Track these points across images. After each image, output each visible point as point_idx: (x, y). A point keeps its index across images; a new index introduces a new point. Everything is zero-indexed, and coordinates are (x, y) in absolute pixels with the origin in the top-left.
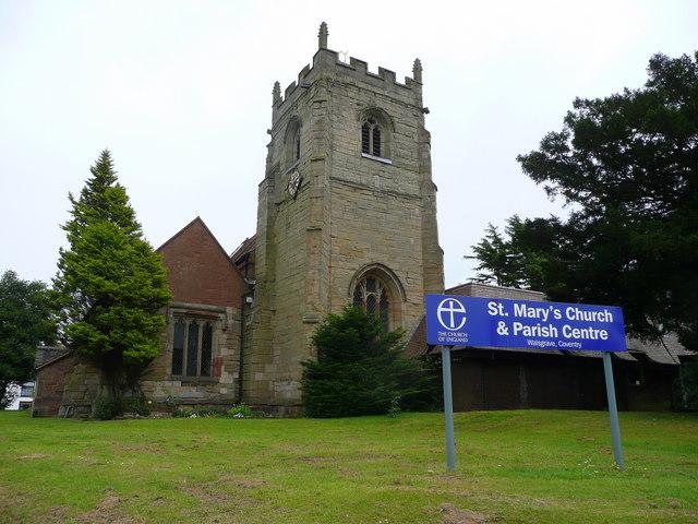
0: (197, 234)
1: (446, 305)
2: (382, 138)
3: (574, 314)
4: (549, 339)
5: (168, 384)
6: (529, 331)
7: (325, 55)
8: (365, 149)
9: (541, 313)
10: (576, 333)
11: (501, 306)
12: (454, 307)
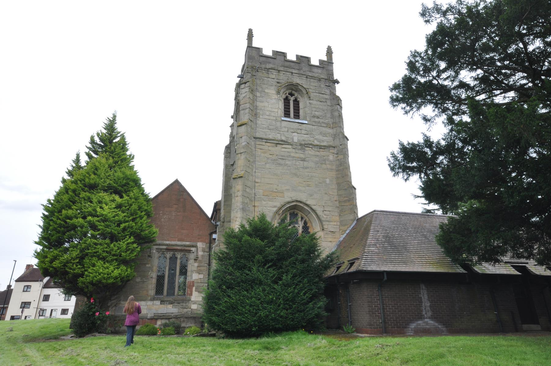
0: (176, 193)
2: (301, 105)
5: (150, 303)
8: (287, 114)
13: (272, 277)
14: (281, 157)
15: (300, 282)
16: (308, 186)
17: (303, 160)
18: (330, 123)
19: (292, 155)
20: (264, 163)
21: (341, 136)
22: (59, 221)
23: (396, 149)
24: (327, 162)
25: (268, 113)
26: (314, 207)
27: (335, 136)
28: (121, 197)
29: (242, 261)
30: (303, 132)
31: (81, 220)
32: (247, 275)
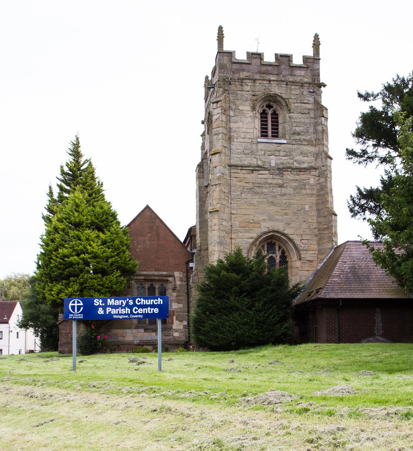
0: (148, 218)
1: (74, 302)
2: (280, 120)
3: (141, 301)
4: (125, 314)
6: (114, 311)
7: (224, 56)
8: (264, 134)
9: (122, 302)
10: (140, 311)
11: (101, 301)
12: (77, 303)
13: (247, 304)
14: (257, 185)
15: (270, 308)
16: (286, 214)
17: (281, 186)
18: (313, 139)
19: (270, 181)
20: (239, 193)
21: (323, 156)
22: (58, 260)
23: (355, 193)
24: (307, 187)
25: (242, 136)
26: (291, 237)
27: (317, 156)
28: (103, 232)
29: (221, 292)
30: (282, 153)
31: (76, 257)
32: (226, 303)
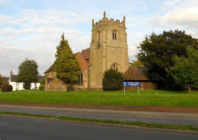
6: (131, 85)
8: (113, 39)
17: (117, 51)
